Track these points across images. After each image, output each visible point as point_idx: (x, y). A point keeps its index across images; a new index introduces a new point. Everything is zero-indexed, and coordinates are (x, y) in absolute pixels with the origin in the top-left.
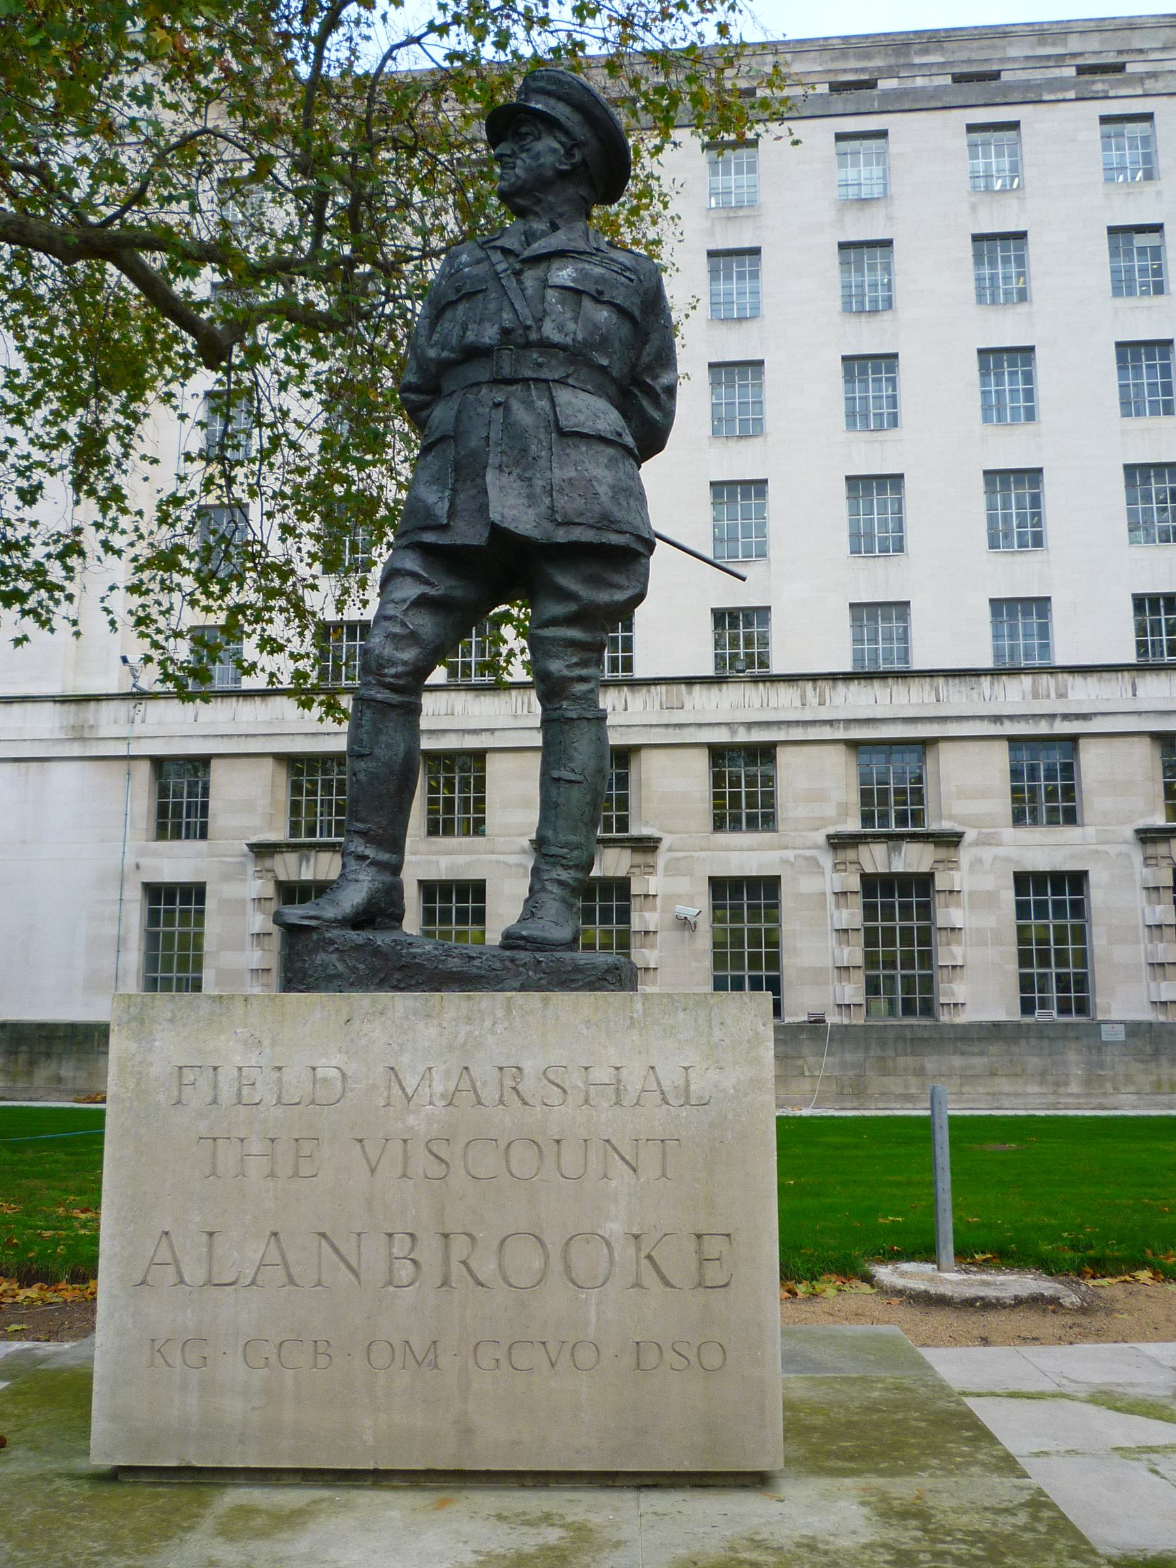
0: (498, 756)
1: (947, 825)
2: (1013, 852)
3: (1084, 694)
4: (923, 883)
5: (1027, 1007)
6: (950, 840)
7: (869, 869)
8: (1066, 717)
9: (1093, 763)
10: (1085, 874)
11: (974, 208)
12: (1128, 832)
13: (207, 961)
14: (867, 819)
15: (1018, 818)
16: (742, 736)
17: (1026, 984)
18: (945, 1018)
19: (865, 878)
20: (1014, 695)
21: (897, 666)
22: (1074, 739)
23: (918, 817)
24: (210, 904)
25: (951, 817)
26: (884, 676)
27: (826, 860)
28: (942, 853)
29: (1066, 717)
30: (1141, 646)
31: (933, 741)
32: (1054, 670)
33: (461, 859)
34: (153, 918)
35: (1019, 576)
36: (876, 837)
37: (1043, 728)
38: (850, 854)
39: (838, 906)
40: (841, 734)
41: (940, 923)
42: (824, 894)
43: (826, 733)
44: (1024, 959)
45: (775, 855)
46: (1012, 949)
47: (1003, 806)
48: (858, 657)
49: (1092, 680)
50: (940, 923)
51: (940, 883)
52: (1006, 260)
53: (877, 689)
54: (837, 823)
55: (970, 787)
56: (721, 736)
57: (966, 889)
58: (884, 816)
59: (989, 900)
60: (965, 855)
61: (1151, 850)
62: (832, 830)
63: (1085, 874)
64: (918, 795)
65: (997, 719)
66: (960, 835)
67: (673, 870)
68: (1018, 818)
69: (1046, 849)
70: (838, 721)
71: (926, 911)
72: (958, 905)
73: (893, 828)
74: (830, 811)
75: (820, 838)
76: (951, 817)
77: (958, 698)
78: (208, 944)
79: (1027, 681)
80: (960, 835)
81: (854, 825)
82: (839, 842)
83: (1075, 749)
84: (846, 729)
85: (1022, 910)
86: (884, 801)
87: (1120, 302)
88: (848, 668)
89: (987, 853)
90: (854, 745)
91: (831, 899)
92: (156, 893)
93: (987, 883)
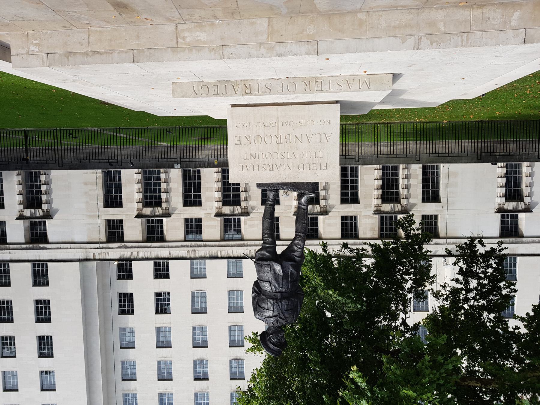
1: (218, 218)
2: (202, 211)
3: (182, 252)
4: (225, 203)
5: (199, 172)
6: (217, 215)
7: (238, 207)
8: (187, 246)
9: (181, 235)
10: (183, 206)
11: (208, 388)
12: (173, 216)
13: (421, 181)
14: (239, 220)
15: (200, 220)
17: (199, 178)
18: (220, 169)
19: (240, 205)
20: (201, 252)
21: (231, 261)
22: (185, 241)
23: (226, 220)
24: (420, 197)
25: (217, 220)
26: (234, 258)
29: (187, 246)
30: (168, 265)
31: (221, 240)
32: (191, 258)
33: (348, 209)
34: (438, 193)
35: (198, 284)
36: (236, 215)
37: (193, 243)
40: (245, 242)
41: (220, 193)
43: (249, 243)
44: (199, 184)
46: (202, 186)
47: (204, 223)
48: (241, 263)
49: (180, 255)
50: (220, 193)
51: (220, 204)
52: (200, 373)
53: (236, 255)
55: (212, 228)
57: (214, 202)
58: (235, 221)
59: (208, 199)
60: (215, 211)
61: (167, 211)
62: (248, 217)
63: (183, 206)
64: (226, 226)
65: (205, 246)
66: (215, 216)
67: (290, 207)
68: (200, 220)
69: (193, 212)
71: (224, 196)
72: (216, 198)
73: (232, 217)
75: (251, 215)
76: (217, 220)
77: (215, 251)
78: (421, 186)
79: (197, 256)
80: (215, 216)
81: (242, 219)
82: (246, 214)
83: (185, 238)
84: (244, 244)
85: (200, 196)
86: (235, 225)
87: (170, 359)
88: (244, 260)
89: (208, 211)
90: (242, 240)
92: (436, 199)
93: (208, 203)
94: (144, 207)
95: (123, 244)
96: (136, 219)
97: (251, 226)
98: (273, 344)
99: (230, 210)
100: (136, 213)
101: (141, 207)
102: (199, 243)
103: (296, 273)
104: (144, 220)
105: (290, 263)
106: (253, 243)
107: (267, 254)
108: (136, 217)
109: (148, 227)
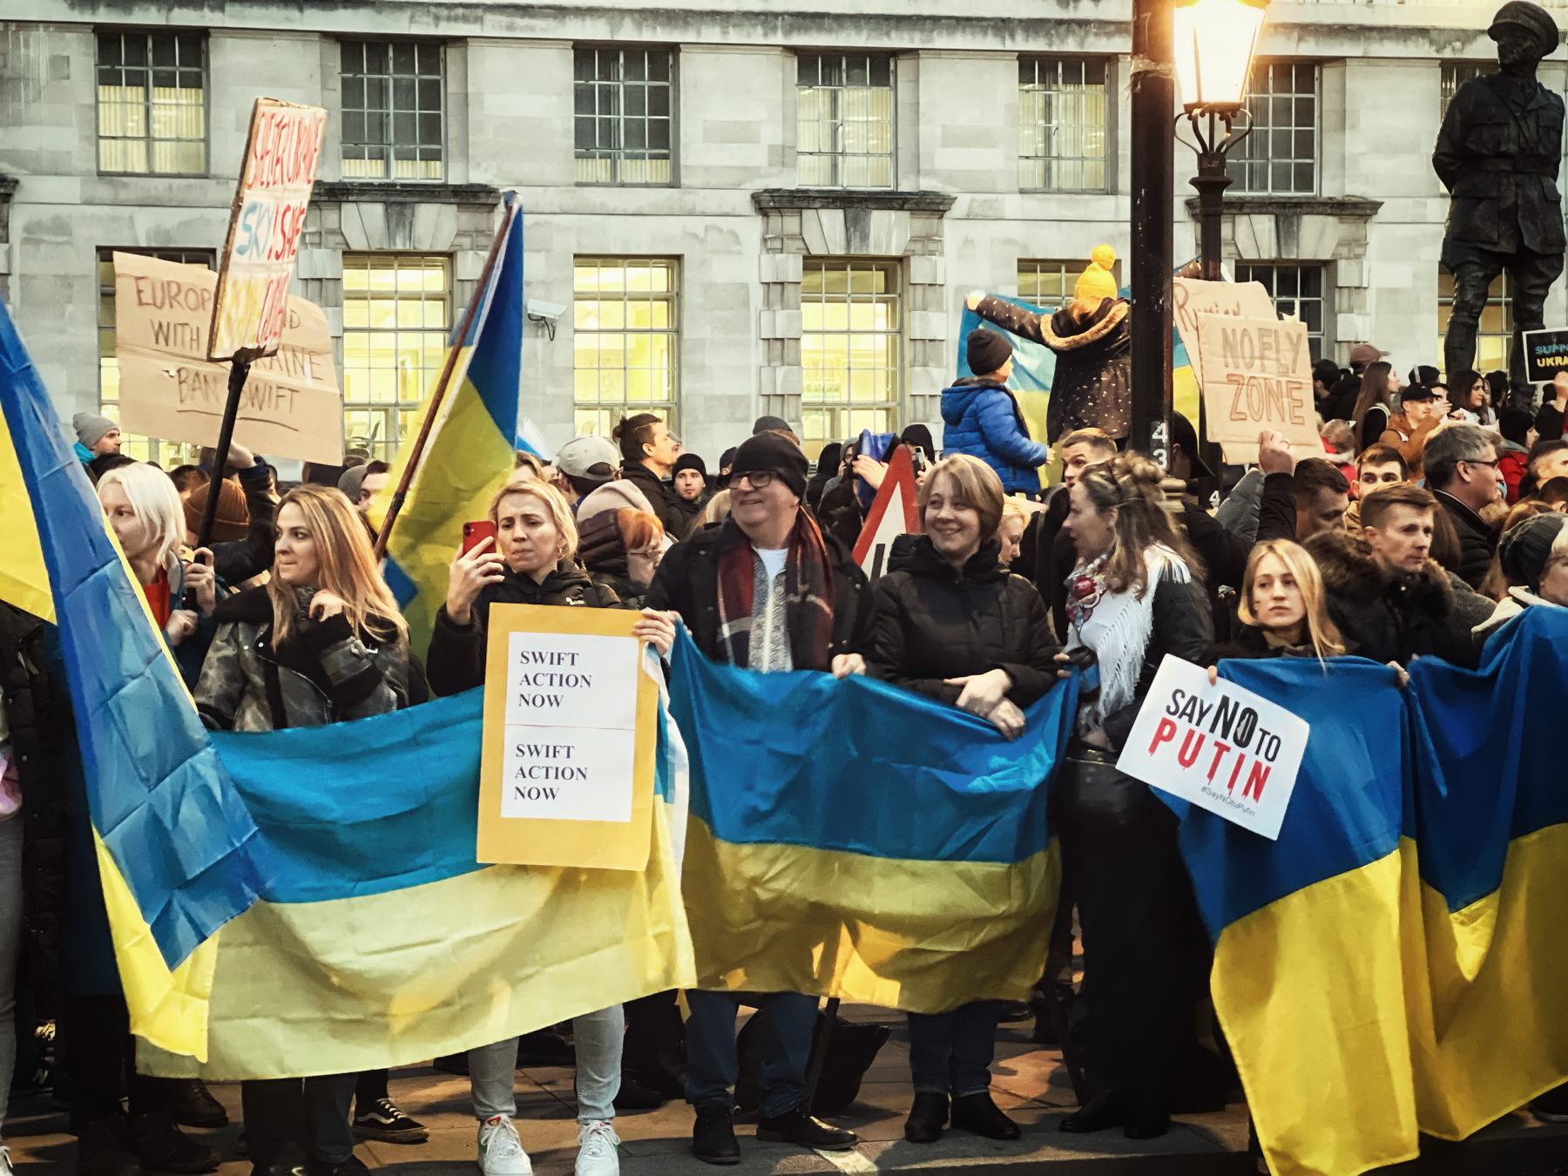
0: (229, 42)
16: (628, 33)
25: (932, 173)
27: (752, 227)
28: (920, 224)
37: (1071, 45)
38: (791, 223)
39: (768, 303)
42: (745, 286)
45: (675, 225)
54: (769, 176)
56: (596, 31)
60: (951, 229)
62: (760, 185)
70: (776, 15)
74: (757, 156)
75: (742, 201)
76: (932, 173)
82: (772, 203)
84: (788, 32)
91: (757, 294)
94: (1330, 264)
95: (1447, 54)
96: (1372, 194)
97: (740, 134)
98: (1530, 31)
99: (864, 237)
100: (1375, 232)
101: (1342, 264)
102: (1037, 45)
103: (1479, 222)
104: (1328, 187)
105: (1496, 249)
106: (734, 36)
107: (1543, 269)
108: (1375, 206)
109: (1306, 145)
